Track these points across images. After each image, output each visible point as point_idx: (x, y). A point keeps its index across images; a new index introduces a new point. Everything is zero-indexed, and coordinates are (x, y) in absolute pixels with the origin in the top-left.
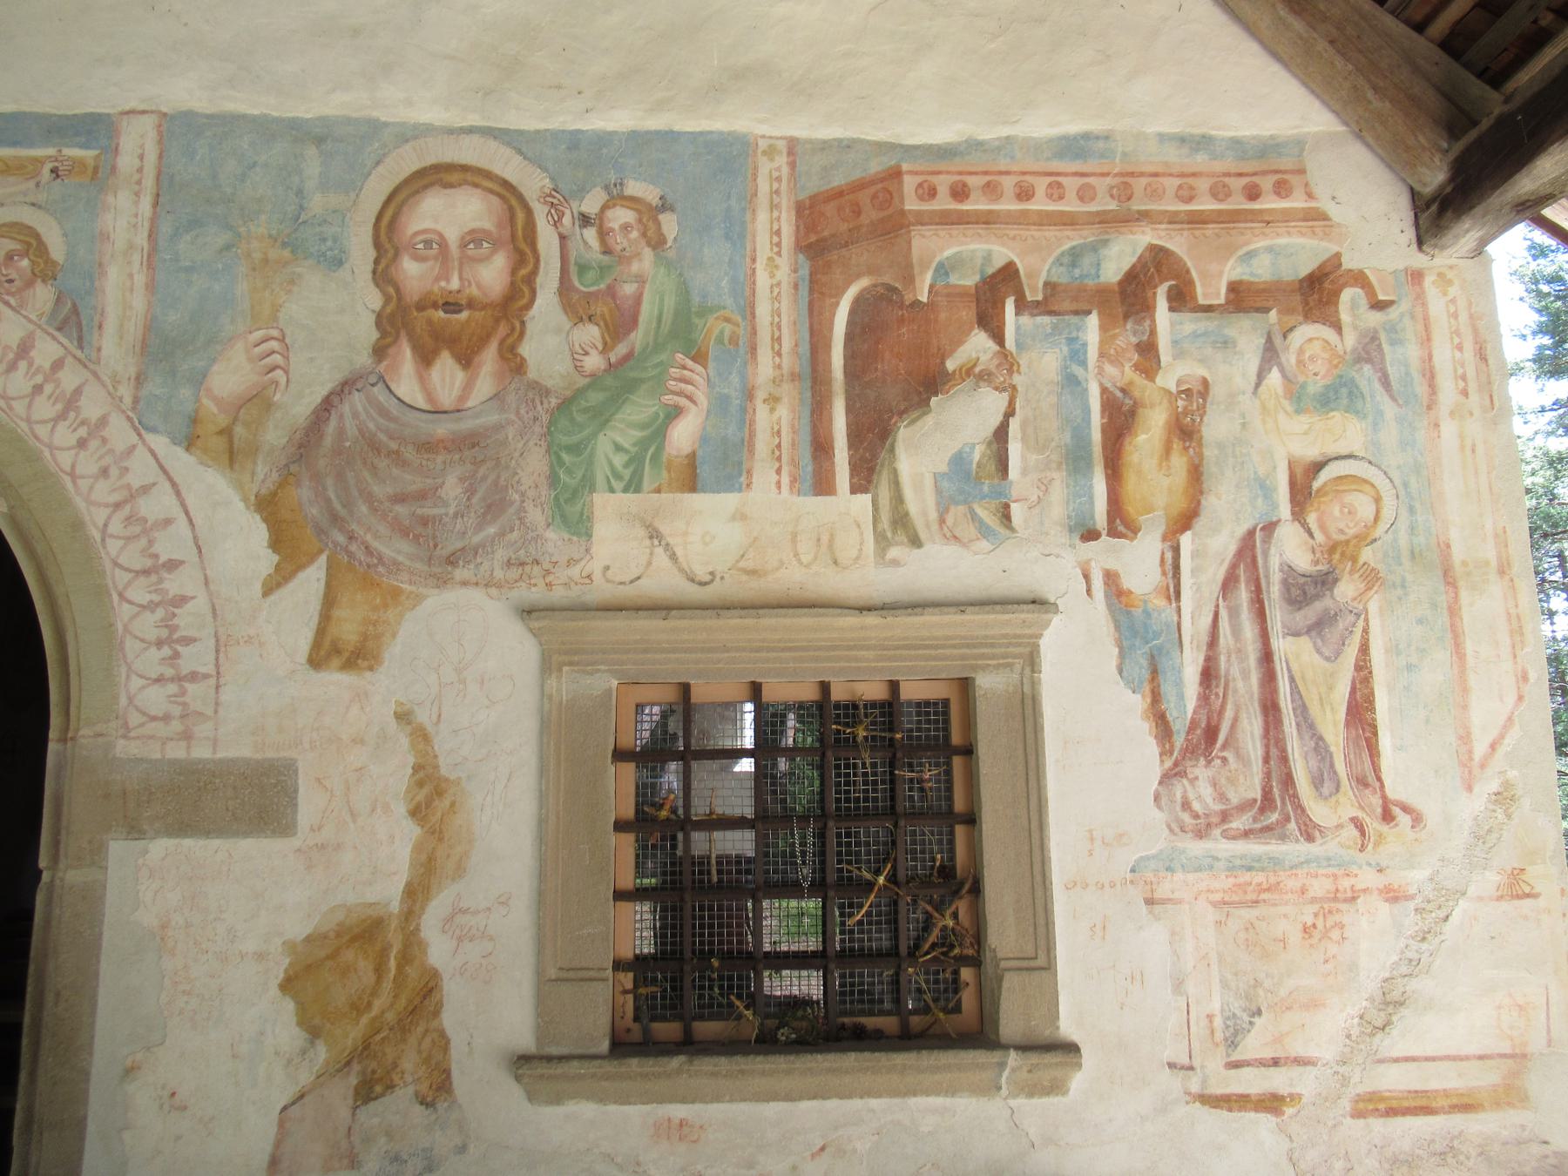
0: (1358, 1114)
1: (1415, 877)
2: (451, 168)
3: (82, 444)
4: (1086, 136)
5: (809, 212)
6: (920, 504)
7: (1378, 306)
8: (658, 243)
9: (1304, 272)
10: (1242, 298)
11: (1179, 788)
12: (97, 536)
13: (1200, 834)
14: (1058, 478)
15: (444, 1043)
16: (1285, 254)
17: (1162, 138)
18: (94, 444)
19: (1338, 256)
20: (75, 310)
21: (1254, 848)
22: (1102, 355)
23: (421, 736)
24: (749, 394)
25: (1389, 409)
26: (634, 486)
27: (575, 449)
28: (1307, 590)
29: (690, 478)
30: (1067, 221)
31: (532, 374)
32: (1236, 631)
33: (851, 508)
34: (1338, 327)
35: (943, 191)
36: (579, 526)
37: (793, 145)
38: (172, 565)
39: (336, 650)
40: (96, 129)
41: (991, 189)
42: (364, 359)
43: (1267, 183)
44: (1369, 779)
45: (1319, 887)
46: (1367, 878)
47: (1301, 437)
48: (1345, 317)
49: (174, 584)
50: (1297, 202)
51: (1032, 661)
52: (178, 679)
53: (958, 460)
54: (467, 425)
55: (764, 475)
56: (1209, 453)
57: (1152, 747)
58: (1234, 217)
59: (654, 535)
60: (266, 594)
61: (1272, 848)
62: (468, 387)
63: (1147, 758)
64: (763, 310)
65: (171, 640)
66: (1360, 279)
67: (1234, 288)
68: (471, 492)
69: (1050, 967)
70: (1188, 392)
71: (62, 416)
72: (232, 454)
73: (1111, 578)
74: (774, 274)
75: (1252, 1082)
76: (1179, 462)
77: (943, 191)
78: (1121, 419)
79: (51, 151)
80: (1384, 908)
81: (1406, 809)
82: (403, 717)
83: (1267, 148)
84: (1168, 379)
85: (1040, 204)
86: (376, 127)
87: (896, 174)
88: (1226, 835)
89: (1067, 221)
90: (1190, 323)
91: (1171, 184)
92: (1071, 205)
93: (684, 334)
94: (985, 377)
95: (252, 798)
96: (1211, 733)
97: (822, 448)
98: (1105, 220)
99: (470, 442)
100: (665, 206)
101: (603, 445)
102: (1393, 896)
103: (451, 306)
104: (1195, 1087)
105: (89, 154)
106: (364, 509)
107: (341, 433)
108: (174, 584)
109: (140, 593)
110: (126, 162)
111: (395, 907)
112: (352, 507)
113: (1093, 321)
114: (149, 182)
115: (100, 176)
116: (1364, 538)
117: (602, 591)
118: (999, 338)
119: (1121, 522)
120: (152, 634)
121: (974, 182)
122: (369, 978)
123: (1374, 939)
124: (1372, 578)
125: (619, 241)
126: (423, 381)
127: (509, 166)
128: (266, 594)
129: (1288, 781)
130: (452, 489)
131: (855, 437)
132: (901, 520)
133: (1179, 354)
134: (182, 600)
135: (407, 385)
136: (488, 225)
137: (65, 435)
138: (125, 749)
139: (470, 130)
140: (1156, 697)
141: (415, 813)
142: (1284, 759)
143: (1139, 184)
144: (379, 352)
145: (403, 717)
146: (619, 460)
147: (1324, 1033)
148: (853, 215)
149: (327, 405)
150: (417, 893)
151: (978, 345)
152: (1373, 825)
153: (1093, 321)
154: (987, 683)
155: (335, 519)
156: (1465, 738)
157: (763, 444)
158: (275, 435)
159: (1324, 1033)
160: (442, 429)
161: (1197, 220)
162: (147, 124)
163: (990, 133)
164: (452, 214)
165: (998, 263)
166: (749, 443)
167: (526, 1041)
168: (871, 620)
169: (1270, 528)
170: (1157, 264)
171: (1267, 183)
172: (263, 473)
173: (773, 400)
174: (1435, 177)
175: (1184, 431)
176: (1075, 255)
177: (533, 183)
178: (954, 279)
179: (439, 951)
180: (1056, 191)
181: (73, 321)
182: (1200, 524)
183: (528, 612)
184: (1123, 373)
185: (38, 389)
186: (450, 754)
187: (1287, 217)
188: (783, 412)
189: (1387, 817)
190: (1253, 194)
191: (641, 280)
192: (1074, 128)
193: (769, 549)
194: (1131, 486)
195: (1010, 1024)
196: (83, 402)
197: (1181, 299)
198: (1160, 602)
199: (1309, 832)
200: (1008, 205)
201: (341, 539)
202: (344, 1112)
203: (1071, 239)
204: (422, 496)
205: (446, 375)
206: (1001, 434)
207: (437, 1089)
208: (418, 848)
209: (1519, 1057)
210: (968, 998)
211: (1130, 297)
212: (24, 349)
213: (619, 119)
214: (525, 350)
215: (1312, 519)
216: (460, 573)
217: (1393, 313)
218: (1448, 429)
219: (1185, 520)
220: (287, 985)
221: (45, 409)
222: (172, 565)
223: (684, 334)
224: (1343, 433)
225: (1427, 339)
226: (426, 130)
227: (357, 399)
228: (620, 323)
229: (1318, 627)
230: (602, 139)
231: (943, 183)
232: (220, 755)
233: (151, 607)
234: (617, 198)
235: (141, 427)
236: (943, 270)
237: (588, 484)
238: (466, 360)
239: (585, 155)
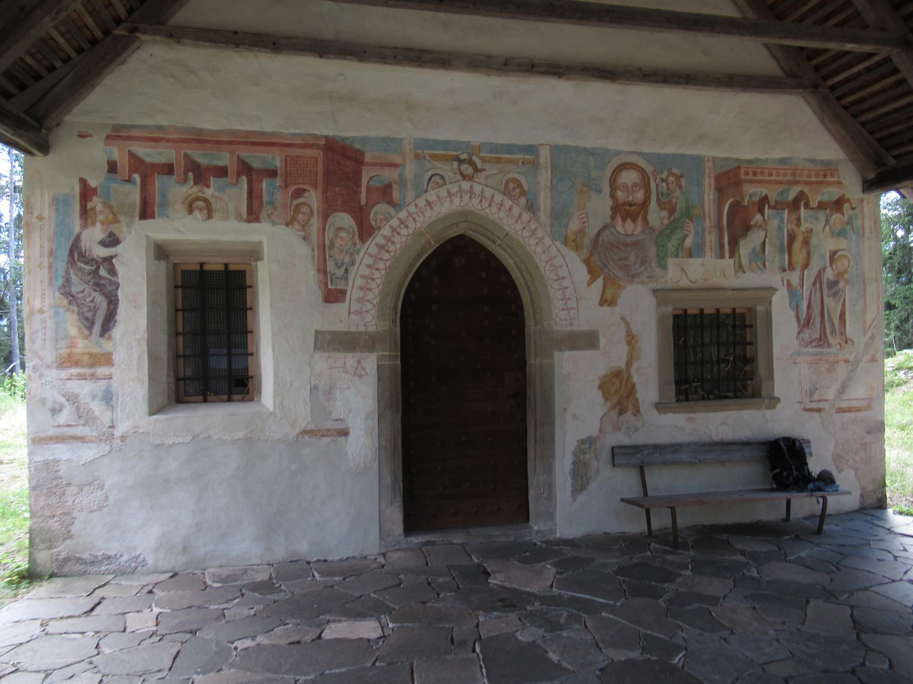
0: (837, 412)
1: (851, 357)
2: (628, 164)
3: (537, 244)
4: (786, 158)
5: (718, 178)
6: (745, 262)
7: (853, 209)
8: (680, 187)
9: (836, 198)
10: (821, 206)
11: (802, 335)
12: (542, 269)
13: (806, 347)
14: (777, 254)
15: (637, 400)
16: (830, 193)
17: (804, 159)
18: (540, 244)
19: (844, 195)
20: (532, 204)
21: (817, 350)
22: (788, 221)
23: (627, 324)
24: (704, 231)
25: (853, 237)
26: (677, 256)
27: (663, 246)
28: (833, 284)
29: (690, 255)
30: (780, 183)
31: (651, 225)
32: (816, 295)
33: (729, 262)
34: (843, 214)
35: (751, 173)
36: (664, 267)
37: (714, 159)
38: (563, 278)
39: (606, 301)
40: (532, 149)
41: (762, 173)
42: (608, 220)
43: (828, 173)
44: (843, 333)
45: (831, 359)
46: (841, 357)
47: (831, 244)
48: (845, 212)
49: (565, 283)
50: (835, 179)
51: (770, 303)
52: (567, 309)
53: (754, 249)
54: (635, 239)
55: (708, 253)
56: (812, 248)
57: (796, 325)
58: (820, 183)
59: (683, 269)
60: (588, 285)
61: (821, 350)
62: (634, 229)
63: (794, 327)
64: (706, 207)
65: (565, 299)
66: (849, 201)
67: (819, 203)
68: (637, 258)
69: (773, 379)
70: (807, 232)
71: (531, 236)
72: (577, 248)
73: (788, 282)
74: (709, 196)
75: (814, 405)
76: (804, 251)
77: (751, 173)
78: (792, 238)
79: (521, 156)
80: (844, 365)
81: (851, 340)
82: (623, 318)
83: (828, 163)
84: (803, 228)
85: (774, 178)
86: (608, 151)
87: (739, 168)
88: (812, 347)
89: (780, 183)
90: (809, 213)
91: (805, 172)
92: (781, 178)
93: (688, 213)
94: (760, 227)
95: (588, 340)
96: (809, 322)
97: (722, 246)
98: (790, 183)
99: (636, 244)
100: (682, 176)
101: (670, 245)
102: (847, 361)
103: (630, 205)
104: (803, 406)
105: (531, 157)
106: (611, 263)
107: (603, 241)
108: (565, 283)
109: (556, 286)
110: (542, 160)
111: (624, 367)
112: (608, 261)
113: (786, 212)
114: (549, 166)
115: (535, 164)
116: (845, 271)
117: (670, 285)
118: (763, 215)
119: (791, 267)
120: (560, 297)
121: (758, 171)
122: (619, 385)
123: (841, 371)
124: (847, 282)
125: (671, 186)
126: (623, 226)
127: (643, 163)
128: (588, 285)
129: (825, 333)
130: (632, 257)
131: (730, 243)
132: (740, 266)
133: (806, 221)
134: (566, 288)
135: (620, 228)
136: (638, 181)
137: (532, 241)
138: (555, 328)
139: (633, 152)
140: (797, 312)
141: (628, 343)
142: (825, 328)
143: (798, 173)
144: (613, 218)
145: (623, 318)
146: (673, 249)
147: (830, 394)
148: (729, 179)
149: (599, 233)
150: (629, 363)
151: (758, 218)
152: (843, 344)
153: (786, 212)
154: (760, 309)
155: (604, 265)
156: (865, 323)
157: (708, 245)
158: (587, 242)
159: (830, 394)
160: (629, 240)
161: (811, 183)
162: (547, 149)
163: (762, 157)
164: (629, 178)
165: (764, 194)
166: (704, 245)
167: (658, 400)
168: (735, 293)
169: (825, 268)
170: (801, 196)
171: (828, 173)
172: (586, 252)
173: (710, 233)
174: (871, 176)
175: (806, 242)
176: (782, 192)
177: (649, 169)
178: (753, 199)
179: (635, 378)
180: (778, 174)
181: (531, 208)
182: (810, 267)
183: (655, 291)
184: (792, 226)
185: (524, 228)
186: (635, 328)
187: (833, 183)
188: (713, 236)
189: (846, 342)
190: (825, 176)
191: (677, 198)
192: (783, 155)
193: (706, 273)
194: (794, 258)
195: (764, 393)
196: (537, 232)
197: (807, 206)
198: (799, 288)
199: (829, 346)
200: (766, 178)
201: (606, 270)
202: (615, 418)
203: (782, 188)
204: (625, 259)
205: (629, 224)
206: (764, 243)
207: (637, 412)
208: (629, 352)
209: (871, 399)
210: (749, 389)
211: (795, 205)
212: (520, 216)
213: (670, 150)
214: (649, 218)
215: (834, 266)
216: (636, 280)
217: (856, 211)
218: (867, 243)
219: (806, 266)
220: (600, 388)
221: (526, 234)
222: (563, 278)
223: (688, 213)
224: (842, 243)
225: (863, 218)
226: (619, 153)
227: (607, 232)
228: (672, 211)
229: (835, 294)
230: (666, 156)
231: (751, 171)
232: (581, 329)
233: (559, 289)
234: (670, 174)
235: (553, 240)
236: (751, 196)
237: (666, 256)
238: (634, 221)
239: (662, 161)
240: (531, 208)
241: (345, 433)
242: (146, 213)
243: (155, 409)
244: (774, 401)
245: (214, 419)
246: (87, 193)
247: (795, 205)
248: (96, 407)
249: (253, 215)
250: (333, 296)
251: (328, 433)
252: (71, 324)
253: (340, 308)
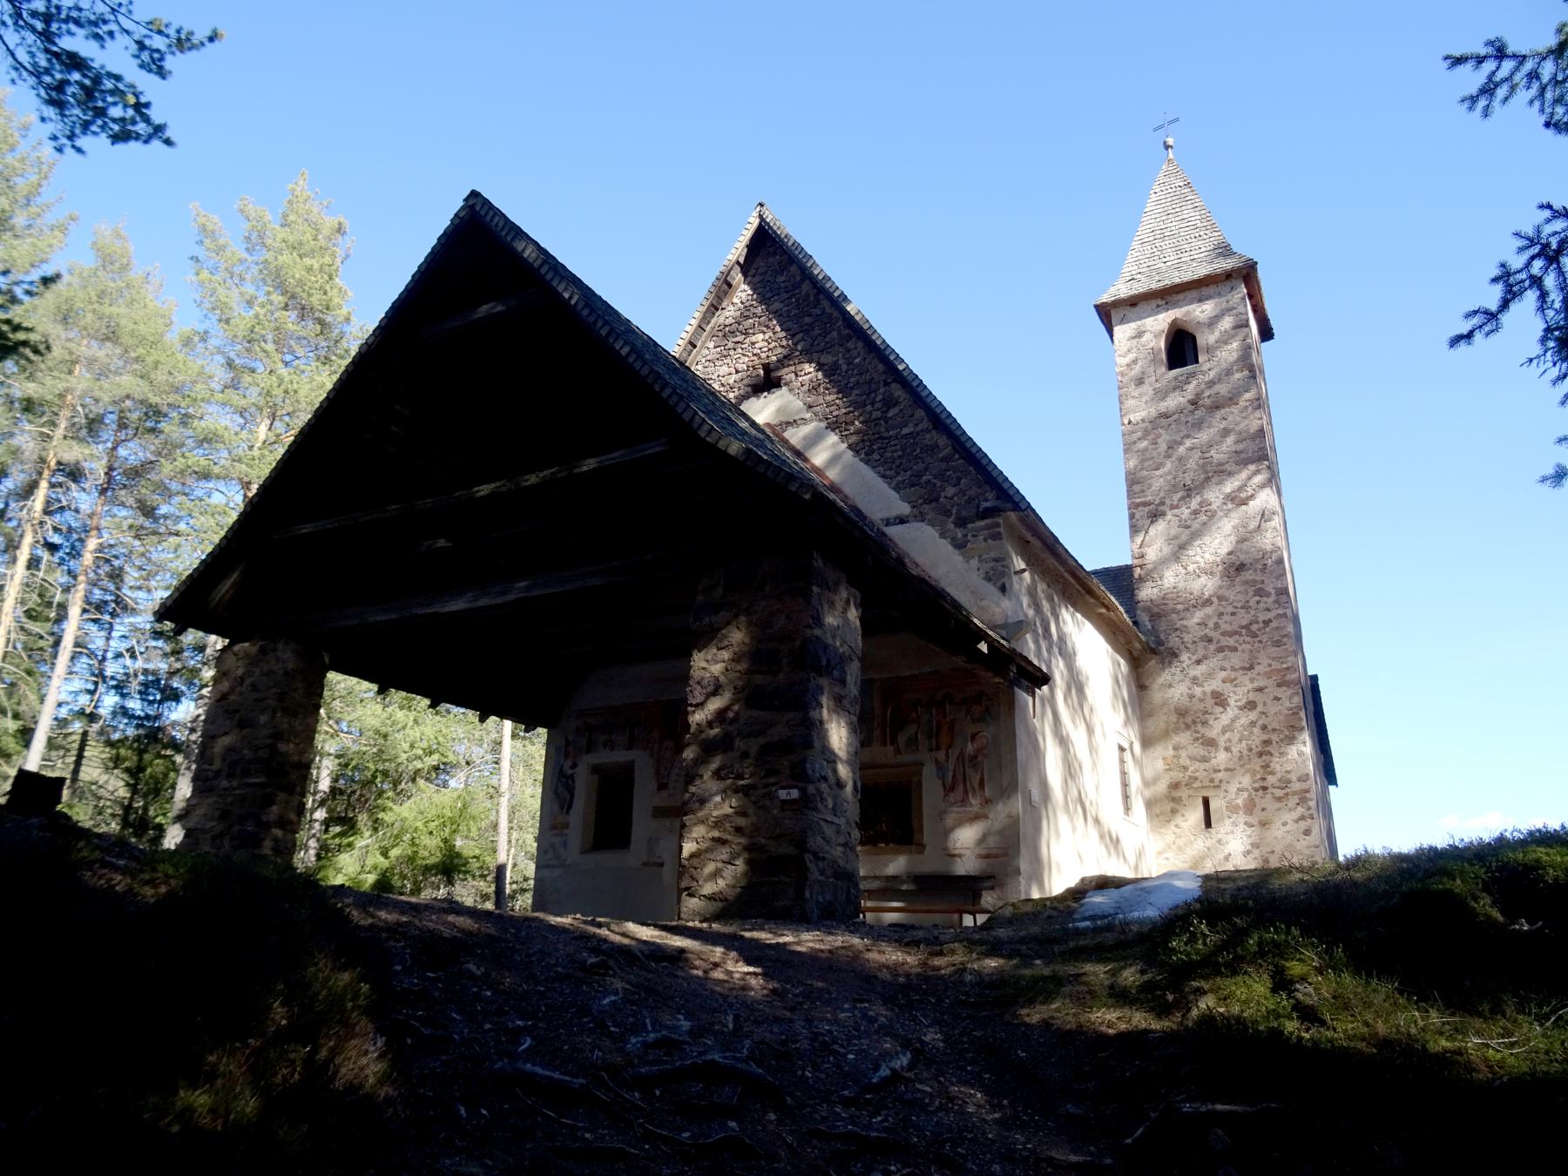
28: (973, 758)
119: (938, 748)
154: (915, 780)
175: (951, 729)
219: (950, 746)
241: (662, 865)
242: (588, 751)
243: (584, 851)
244: (921, 847)
245: (607, 858)
246: (568, 743)
248: (561, 850)
249: (629, 748)
250: (662, 787)
251: (654, 864)
252: (556, 807)
253: (664, 793)
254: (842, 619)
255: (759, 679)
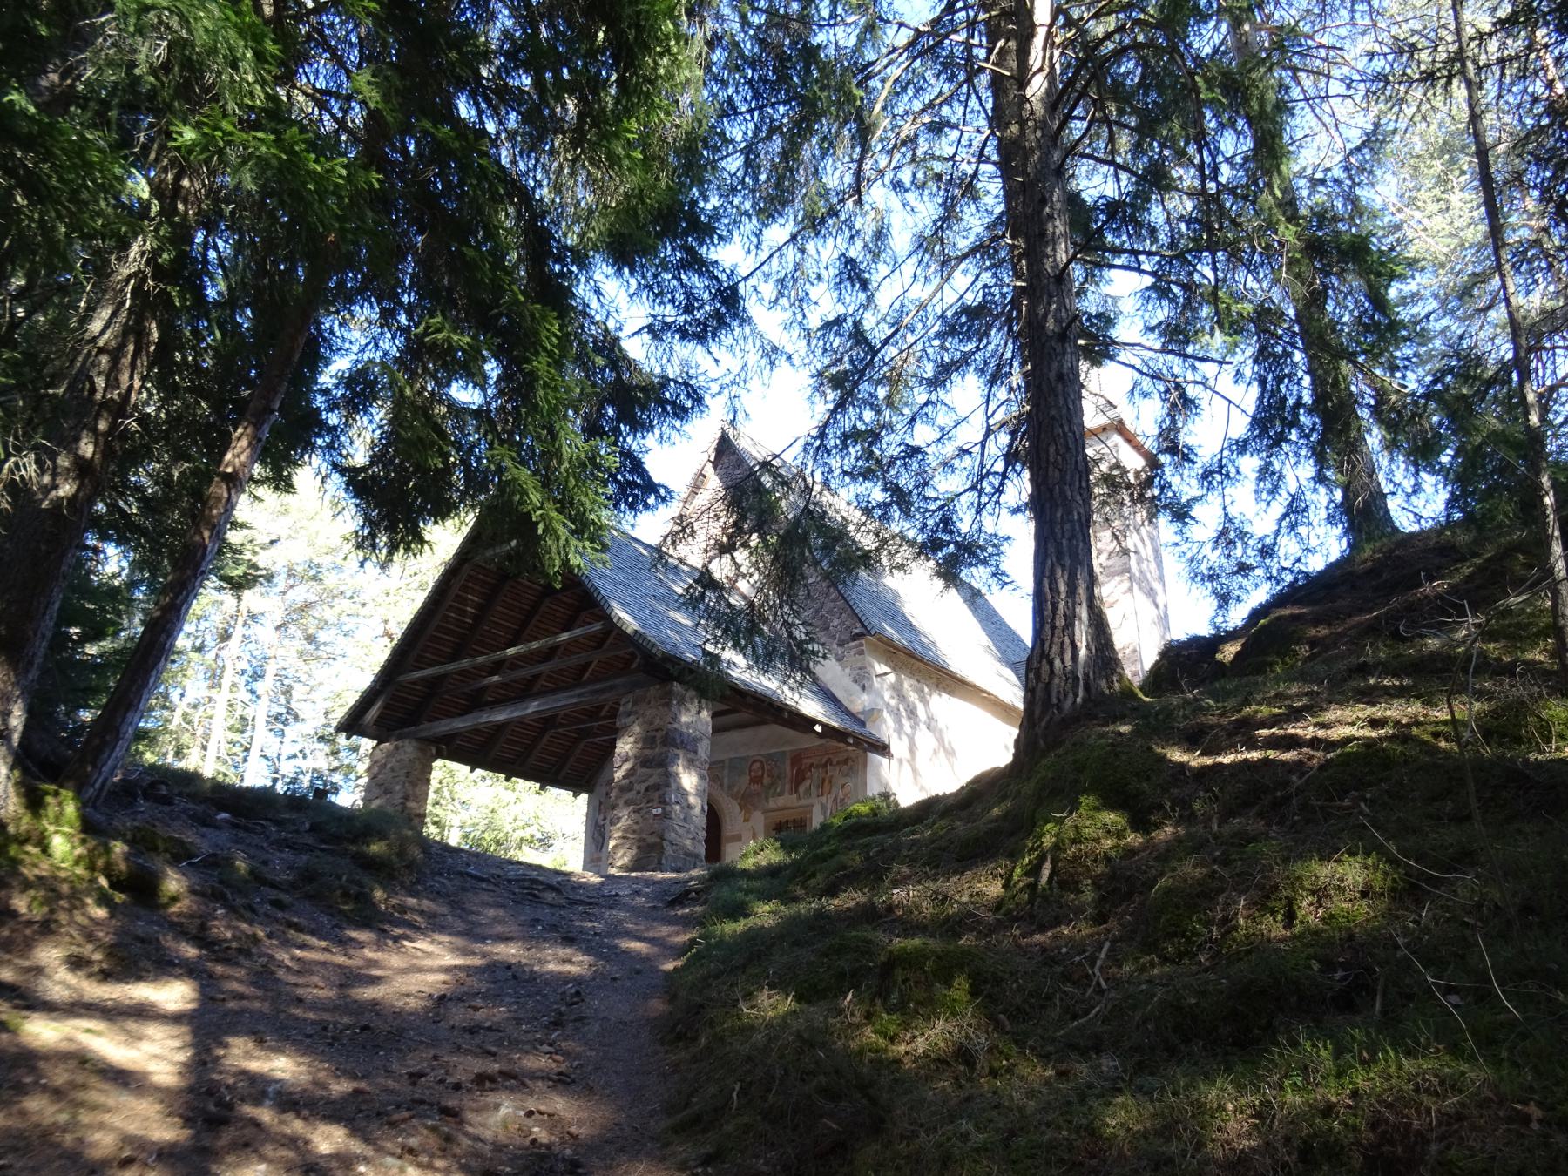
74: (788, 768)
148: (797, 759)
164: (757, 765)
181: (721, 785)
239: (770, 757)
240: (721, 785)
247: (825, 766)
254: (695, 718)
255: (647, 752)
